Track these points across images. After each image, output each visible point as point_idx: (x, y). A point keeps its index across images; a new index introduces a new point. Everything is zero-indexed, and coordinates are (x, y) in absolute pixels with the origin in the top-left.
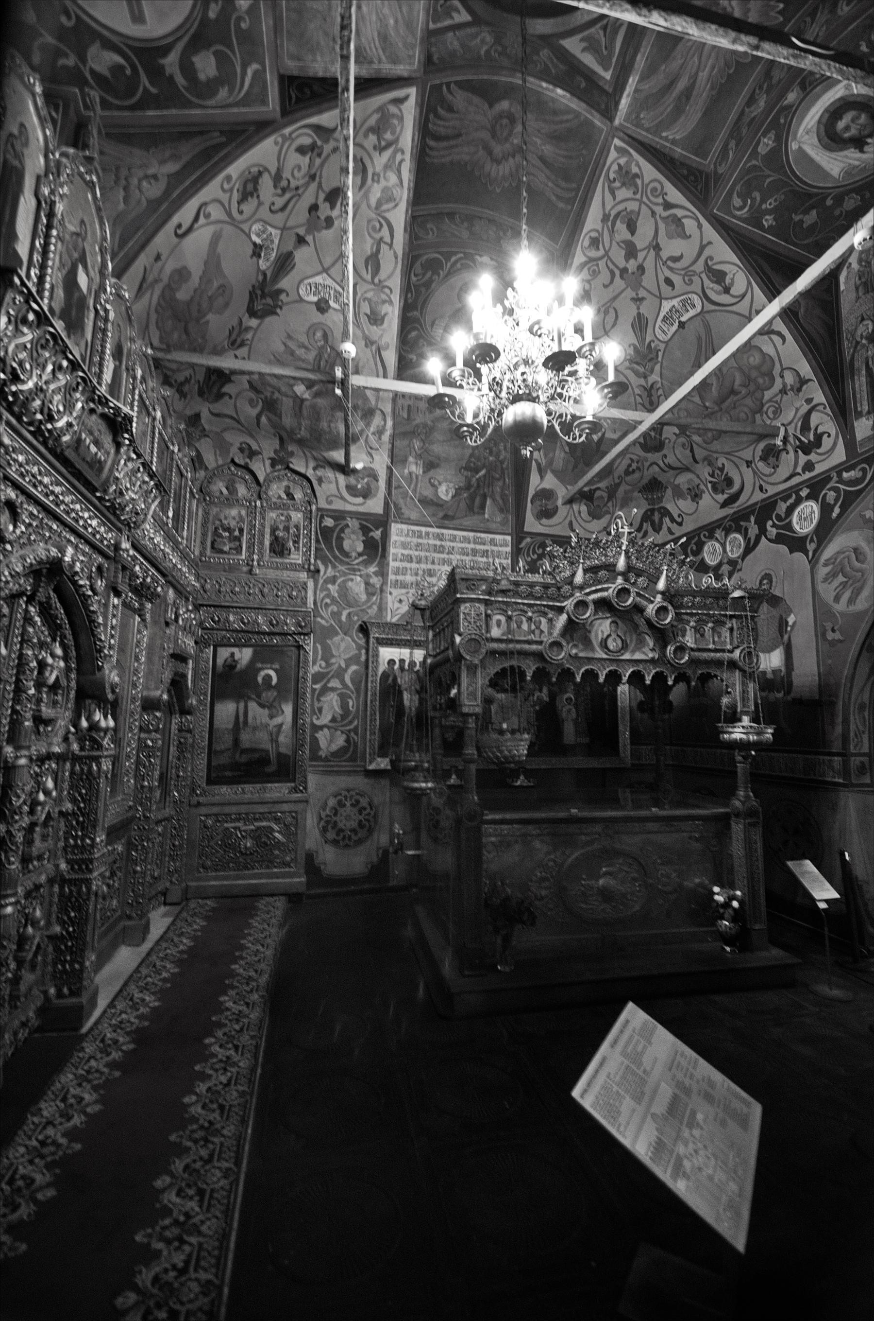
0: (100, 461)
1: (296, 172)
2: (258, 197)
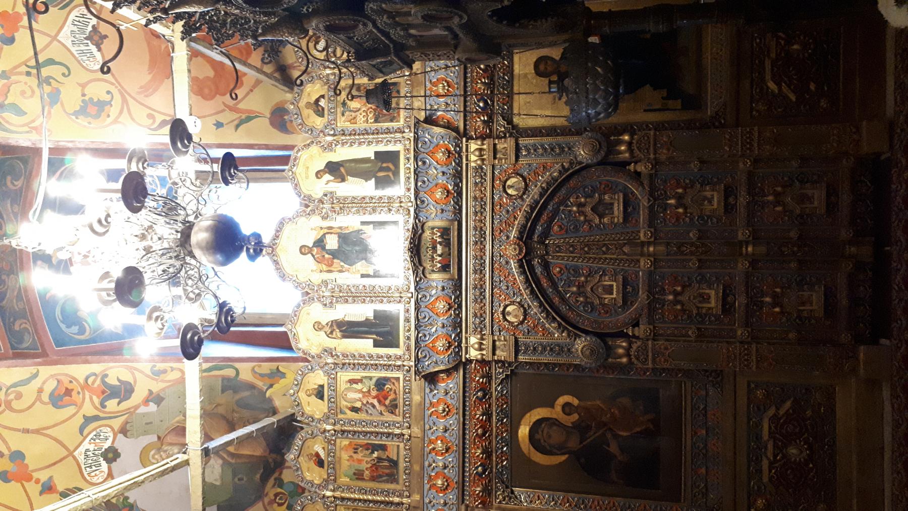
0: (441, 236)
1: (29, 93)
2: (84, 95)
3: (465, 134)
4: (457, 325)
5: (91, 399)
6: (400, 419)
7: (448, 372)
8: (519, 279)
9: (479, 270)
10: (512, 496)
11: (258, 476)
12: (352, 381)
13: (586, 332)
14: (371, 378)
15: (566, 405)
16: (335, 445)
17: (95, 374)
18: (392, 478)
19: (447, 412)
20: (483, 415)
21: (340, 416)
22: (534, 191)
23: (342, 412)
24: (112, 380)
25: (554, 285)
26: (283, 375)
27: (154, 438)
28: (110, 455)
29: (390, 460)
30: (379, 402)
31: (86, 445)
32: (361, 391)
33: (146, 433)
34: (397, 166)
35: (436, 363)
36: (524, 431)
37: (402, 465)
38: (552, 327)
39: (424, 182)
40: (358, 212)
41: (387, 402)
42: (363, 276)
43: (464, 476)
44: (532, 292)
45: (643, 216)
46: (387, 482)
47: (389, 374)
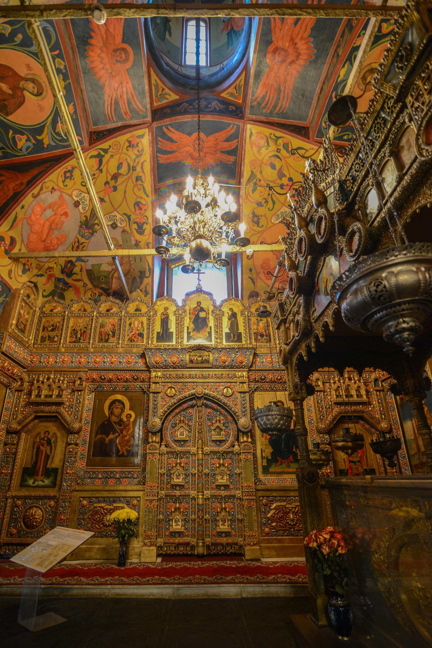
0: (205, 360)
1: (261, 194)
2: (261, 216)
3: (250, 370)
4: (166, 367)
5: (137, 218)
6: (126, 343)
7: (146, 363)
8: (187, 394)
9: (190, 377)
10: (91, 391)
11: (103, 286)
12: (142, 323)
13: (163, 424)
14: (143, 331)
15: (131, 416)
16: (116, 316)
17: (148, 219)
18: (101, 340)
19: (128, 363)
20: (127, 379)
21: (128, 318)
22: (225, 400)
23: (129, 319)
24: (145, 226)
25: (184, 410)
26: (146, 296)
27: (121, 243)
28: (114, 226)
29: (108, 339)
30: (133, 335)
31: (119, 216)
32: (138, 326)
33: (123, 240)
34: (235, 342)
35: (149, 358)
36: (119, 397)
37: (106, 344)
38: (165, 408)
39: (229, 352)
40: (215, 325)
41: (133, 338)
42: (188, 327)
43: (100, 370)
44: (181, 400)
45: (216, 449)
46: (99, 338)
47: (145, 338)
